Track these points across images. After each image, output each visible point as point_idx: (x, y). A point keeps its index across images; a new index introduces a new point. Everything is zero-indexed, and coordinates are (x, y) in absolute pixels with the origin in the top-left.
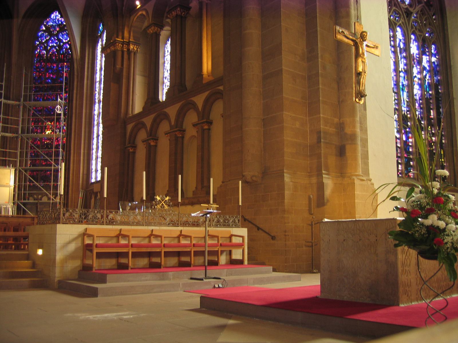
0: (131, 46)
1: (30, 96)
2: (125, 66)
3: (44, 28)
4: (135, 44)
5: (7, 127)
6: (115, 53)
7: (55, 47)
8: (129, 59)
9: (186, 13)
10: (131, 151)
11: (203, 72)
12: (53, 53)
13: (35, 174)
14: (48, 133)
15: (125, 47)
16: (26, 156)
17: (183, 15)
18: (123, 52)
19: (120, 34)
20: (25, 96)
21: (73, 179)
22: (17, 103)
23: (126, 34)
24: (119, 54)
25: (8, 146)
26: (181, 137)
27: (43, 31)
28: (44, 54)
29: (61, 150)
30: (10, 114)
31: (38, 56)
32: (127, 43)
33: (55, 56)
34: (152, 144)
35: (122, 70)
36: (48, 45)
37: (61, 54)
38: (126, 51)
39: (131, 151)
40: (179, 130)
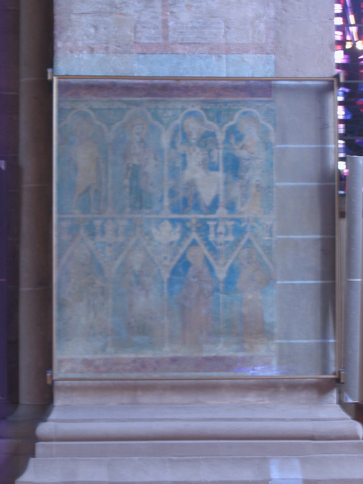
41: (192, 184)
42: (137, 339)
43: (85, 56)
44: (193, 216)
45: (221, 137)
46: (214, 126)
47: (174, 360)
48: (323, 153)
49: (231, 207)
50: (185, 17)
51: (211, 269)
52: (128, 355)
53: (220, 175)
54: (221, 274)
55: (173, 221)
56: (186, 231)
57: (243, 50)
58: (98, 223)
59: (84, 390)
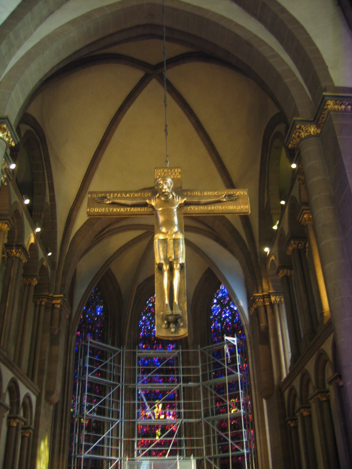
0: (272, 298)
1: (210, 373)
2: (270, 322)
4: (275, 294)
5: (192, 412)
6: (257, 310)
7: (228, 317)
8: (273, 313)
9: (303, 243)
10: (292, 425)
11: (324, 309)
12: (227, 323)
13: (226, 462)
14: (234, 411)
15: (266, 301)
16: (214, 442)
17: (301, 246)
18: (265, 306)
19: (260, 288)
20: (203, 375)
21: (262, 464)
22: (196, 384)
23: (265, 286)
24: (262, 310)
25: (194, 433)
26: (325, 401)
28: (218, 327)
29: (244, 430)
30: (193, 397)
31: (214, 331)
32: (268, 296)
33: (229, 326)
34: (305, 414)
35: (267, 327)
36: (221, 317)
37: (235, 323)
38: (268, 305)
39: (292, 425)
40: (319, 392)
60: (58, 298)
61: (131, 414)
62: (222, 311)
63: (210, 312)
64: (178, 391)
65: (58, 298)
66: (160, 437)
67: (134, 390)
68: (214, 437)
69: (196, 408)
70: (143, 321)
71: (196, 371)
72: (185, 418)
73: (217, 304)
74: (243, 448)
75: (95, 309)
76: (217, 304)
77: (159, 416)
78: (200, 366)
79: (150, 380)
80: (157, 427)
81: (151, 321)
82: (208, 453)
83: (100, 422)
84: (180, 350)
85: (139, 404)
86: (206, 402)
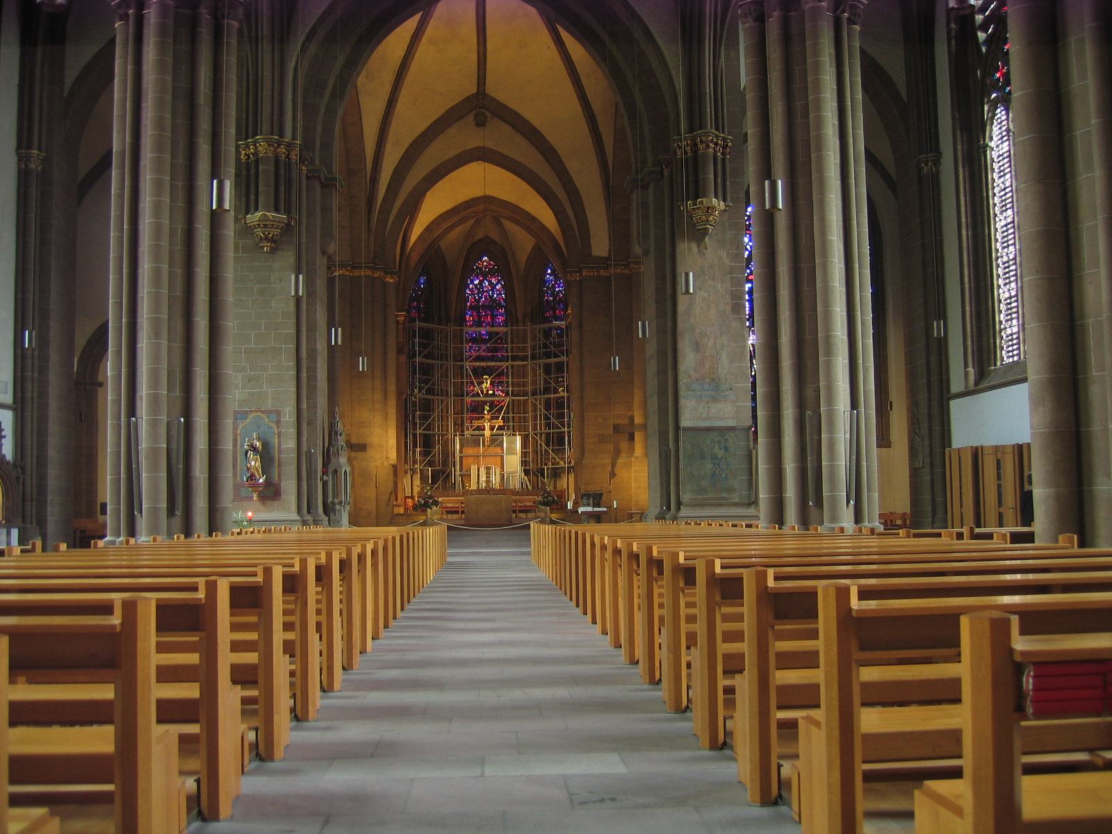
3: (549, 271)
27: (549, 274)
36: (554, 290)
41: (715, 453)
42: (704, 493)
43: (688, 421)
44: (716, 462)
45: (723, 441)
46: (720, 438)
47: (712, 498)
48: (749, 445)
49: (725, 459)
50: (713, 411)
51: (721, 475)
52: (701, 497)
53: (723, 451)
54: (724, 476)
55: (711, 463)
56: (714, 465)
57: (728, 419)
58: (692, 464)
59: (690, 506)
60: (401, 316)
61: (460, 394)
62: (556, 283)
63: (544, 282)
64: (507, 367)
65: (401, 316)
66: (488, 411)
67: (462, 367)
68: (540, 415)
69: (524, 386)
70: (470, 290)
71: (524, 349)
72: (513, 395)
73: (550, 275)
74: (564, 427)
75: (418, 282)
76: (550, 275)
77: (488, 391)
78: (529, 344)
79: (479, 359)
80: (484, 403)
81: (478, 290)
82: (535, 428)
83: (430, 399)
84: (510, 328)
85: (467, 382)
86: (534, 382)
